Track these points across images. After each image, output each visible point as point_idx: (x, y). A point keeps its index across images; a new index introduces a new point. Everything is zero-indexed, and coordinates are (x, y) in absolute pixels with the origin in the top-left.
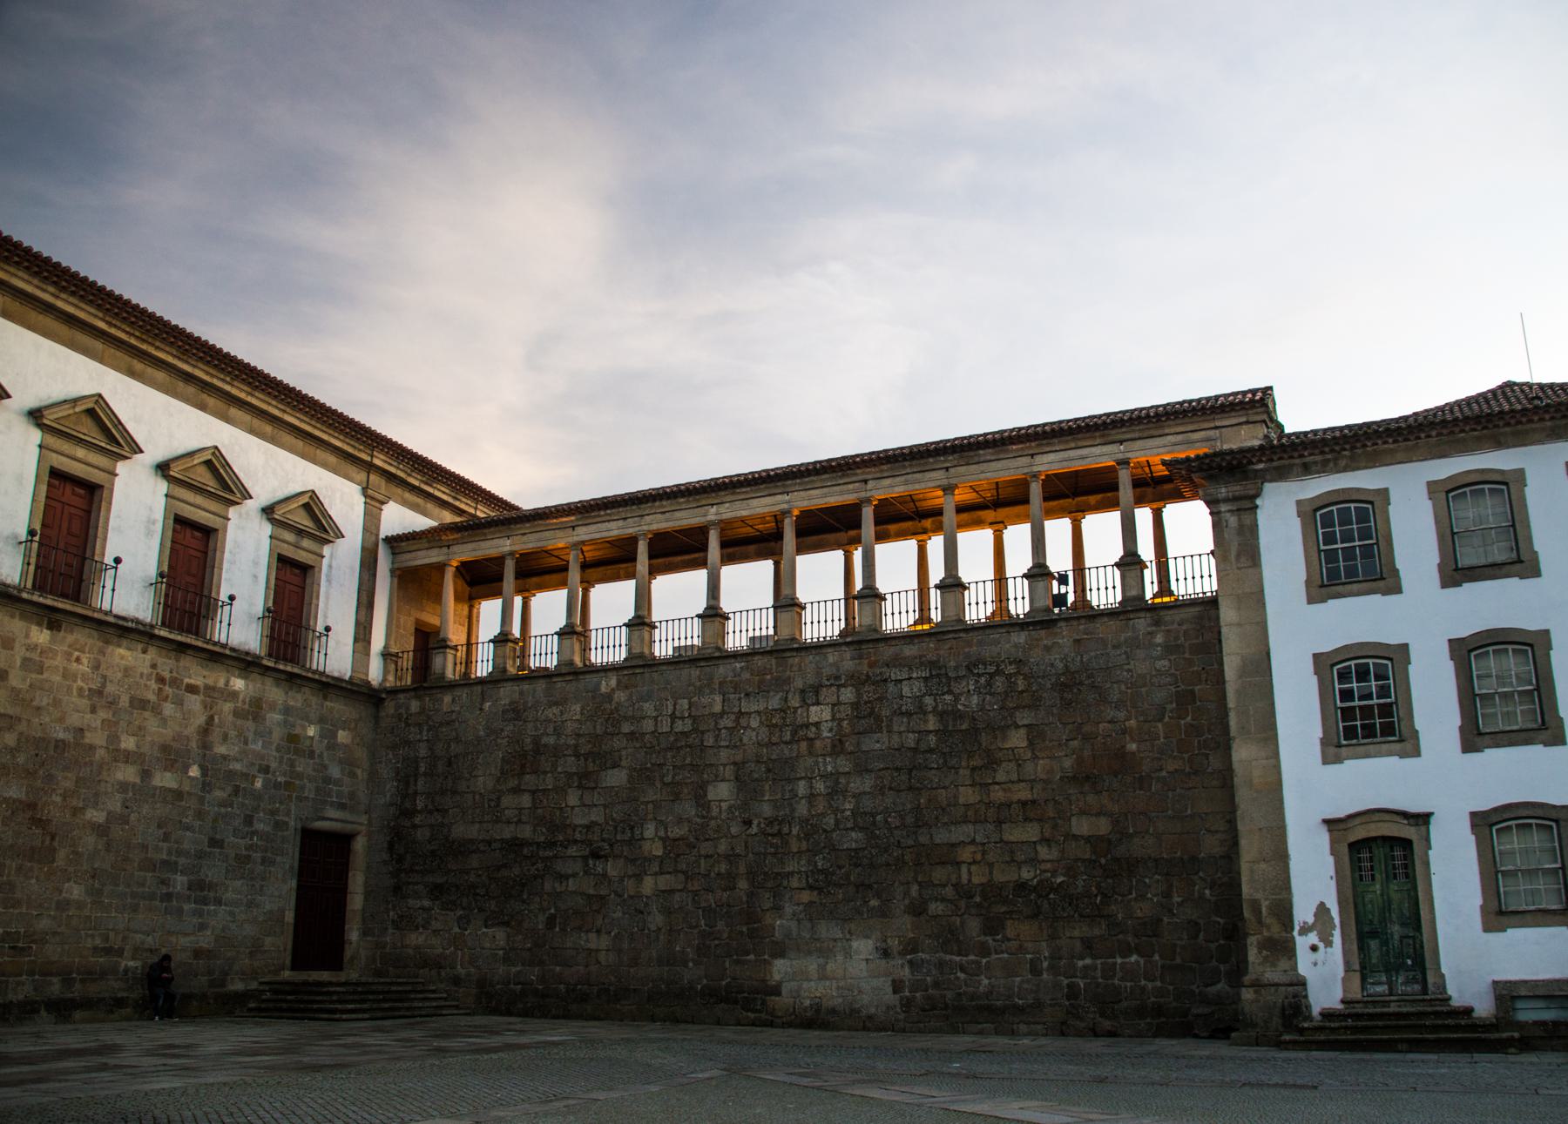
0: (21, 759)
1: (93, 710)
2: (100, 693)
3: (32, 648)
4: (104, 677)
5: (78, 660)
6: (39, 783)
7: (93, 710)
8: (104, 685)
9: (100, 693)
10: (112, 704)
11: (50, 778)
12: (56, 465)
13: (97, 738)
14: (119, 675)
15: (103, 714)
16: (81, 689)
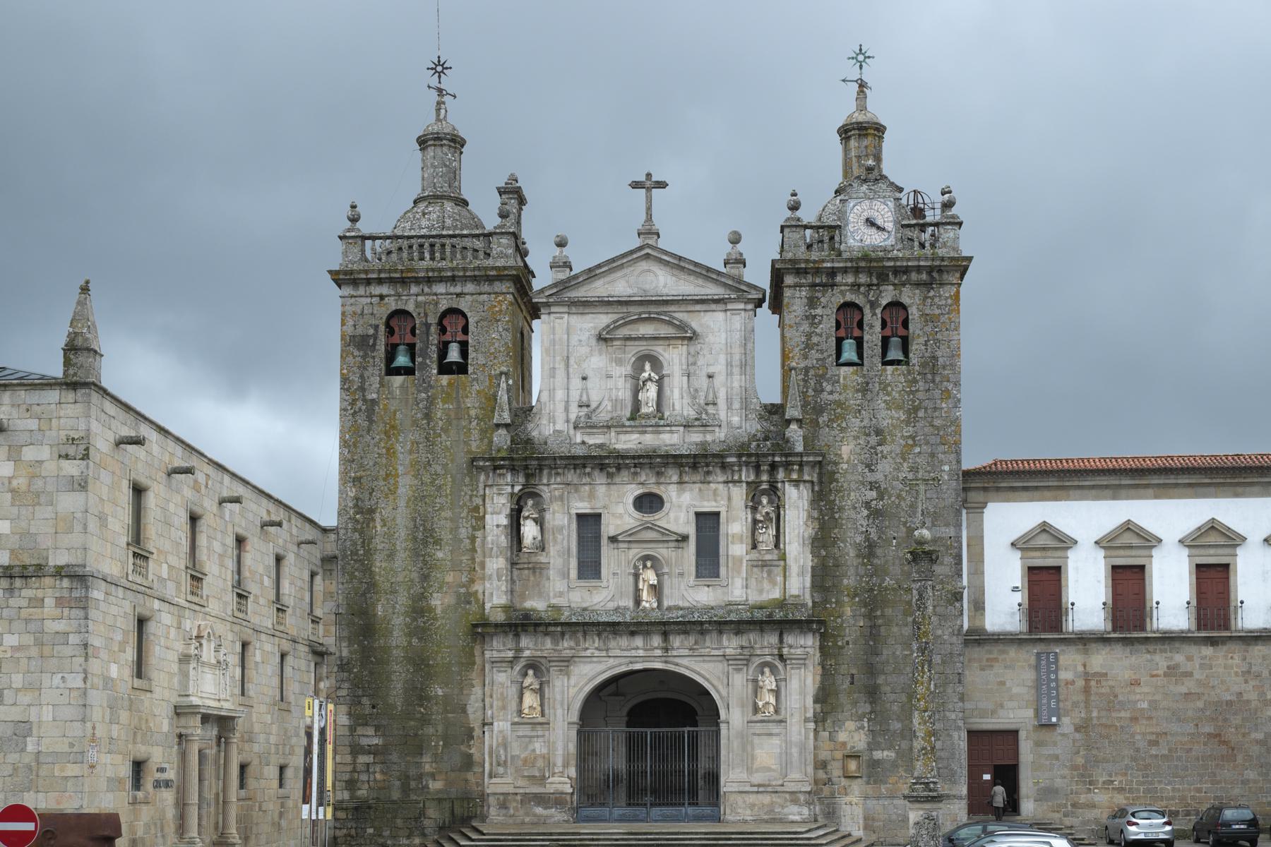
0: (1208, 713)
1: (1246, 682)
2: (1249, 672)
3: (1203, 658)
4: (1250, 664)
5: (1232, 658)
6: (1220, 723)
7: (1246, 682)
8: (1251, 668)
9: (1249, 672)
10: (1258, 676)
11: (1225, 720)
12: (1199, 562)
13: (1253, 696)
14: (1260, 661)
15: (1252, 683)
16: (1236, 673)
